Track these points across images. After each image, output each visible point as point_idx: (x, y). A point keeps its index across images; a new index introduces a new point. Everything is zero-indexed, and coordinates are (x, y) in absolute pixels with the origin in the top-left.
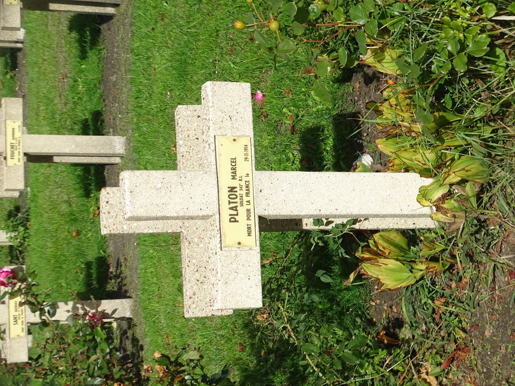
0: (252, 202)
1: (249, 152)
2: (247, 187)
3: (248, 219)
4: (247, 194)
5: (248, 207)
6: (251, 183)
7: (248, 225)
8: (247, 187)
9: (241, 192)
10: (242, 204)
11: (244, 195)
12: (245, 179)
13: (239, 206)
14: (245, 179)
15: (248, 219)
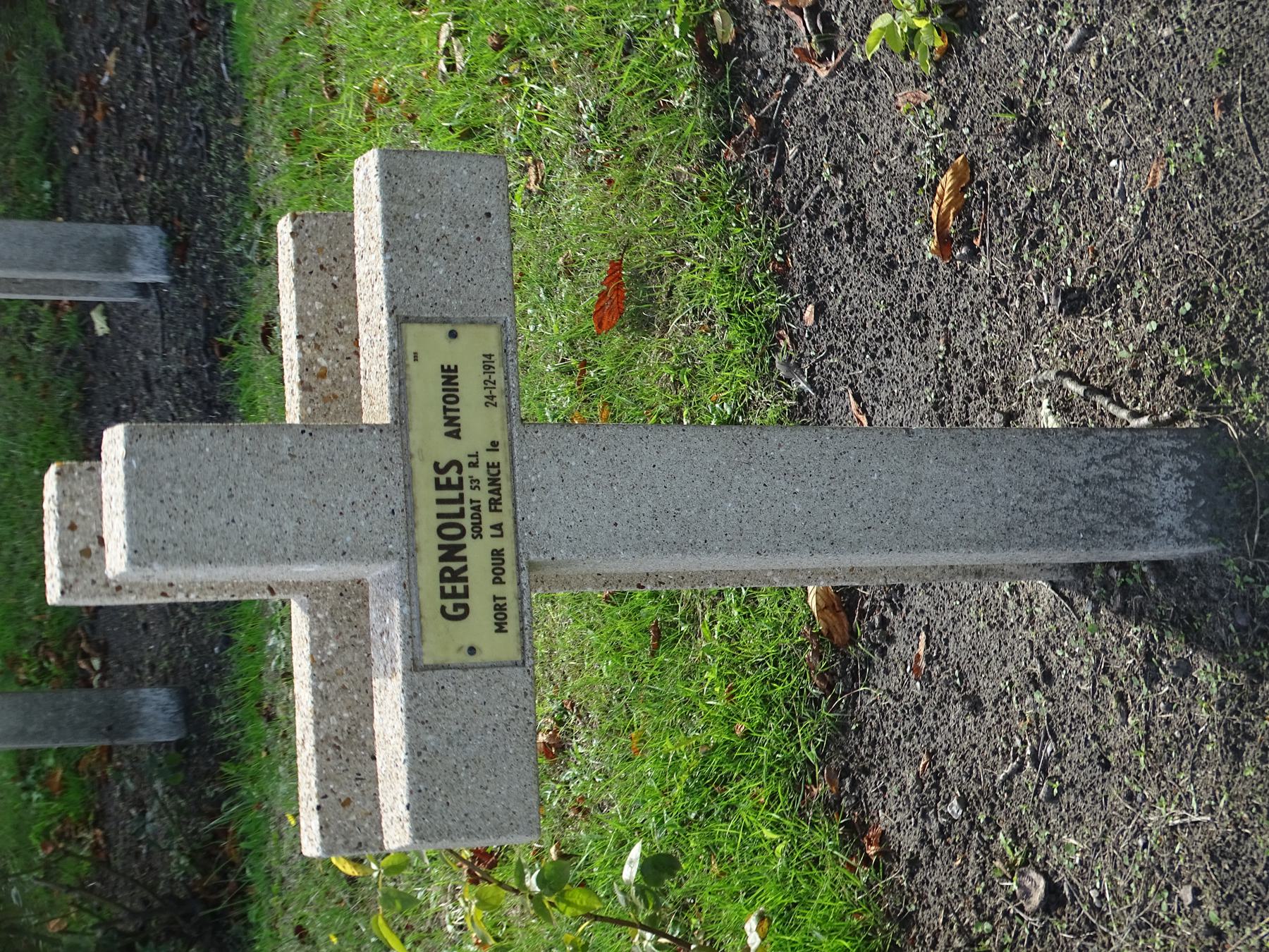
0: (508, 528)
1: (498, 376)
2: (494, 481)
3: (498, 580)
4: (495, 505)
5: (497, 544)
6: (505, 469)
7: (495, 598)
8: (494, 481)
9: (475, 495)
10: (478, 534)
11: (485, 506)
12: (485, 458)
13: (467, 539)
14: (485, 458)
15: (498, 580)
